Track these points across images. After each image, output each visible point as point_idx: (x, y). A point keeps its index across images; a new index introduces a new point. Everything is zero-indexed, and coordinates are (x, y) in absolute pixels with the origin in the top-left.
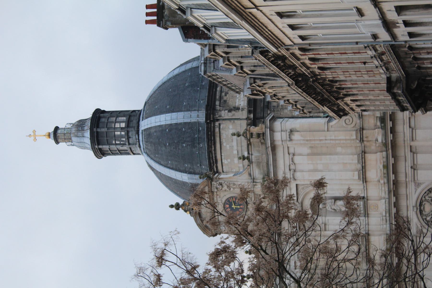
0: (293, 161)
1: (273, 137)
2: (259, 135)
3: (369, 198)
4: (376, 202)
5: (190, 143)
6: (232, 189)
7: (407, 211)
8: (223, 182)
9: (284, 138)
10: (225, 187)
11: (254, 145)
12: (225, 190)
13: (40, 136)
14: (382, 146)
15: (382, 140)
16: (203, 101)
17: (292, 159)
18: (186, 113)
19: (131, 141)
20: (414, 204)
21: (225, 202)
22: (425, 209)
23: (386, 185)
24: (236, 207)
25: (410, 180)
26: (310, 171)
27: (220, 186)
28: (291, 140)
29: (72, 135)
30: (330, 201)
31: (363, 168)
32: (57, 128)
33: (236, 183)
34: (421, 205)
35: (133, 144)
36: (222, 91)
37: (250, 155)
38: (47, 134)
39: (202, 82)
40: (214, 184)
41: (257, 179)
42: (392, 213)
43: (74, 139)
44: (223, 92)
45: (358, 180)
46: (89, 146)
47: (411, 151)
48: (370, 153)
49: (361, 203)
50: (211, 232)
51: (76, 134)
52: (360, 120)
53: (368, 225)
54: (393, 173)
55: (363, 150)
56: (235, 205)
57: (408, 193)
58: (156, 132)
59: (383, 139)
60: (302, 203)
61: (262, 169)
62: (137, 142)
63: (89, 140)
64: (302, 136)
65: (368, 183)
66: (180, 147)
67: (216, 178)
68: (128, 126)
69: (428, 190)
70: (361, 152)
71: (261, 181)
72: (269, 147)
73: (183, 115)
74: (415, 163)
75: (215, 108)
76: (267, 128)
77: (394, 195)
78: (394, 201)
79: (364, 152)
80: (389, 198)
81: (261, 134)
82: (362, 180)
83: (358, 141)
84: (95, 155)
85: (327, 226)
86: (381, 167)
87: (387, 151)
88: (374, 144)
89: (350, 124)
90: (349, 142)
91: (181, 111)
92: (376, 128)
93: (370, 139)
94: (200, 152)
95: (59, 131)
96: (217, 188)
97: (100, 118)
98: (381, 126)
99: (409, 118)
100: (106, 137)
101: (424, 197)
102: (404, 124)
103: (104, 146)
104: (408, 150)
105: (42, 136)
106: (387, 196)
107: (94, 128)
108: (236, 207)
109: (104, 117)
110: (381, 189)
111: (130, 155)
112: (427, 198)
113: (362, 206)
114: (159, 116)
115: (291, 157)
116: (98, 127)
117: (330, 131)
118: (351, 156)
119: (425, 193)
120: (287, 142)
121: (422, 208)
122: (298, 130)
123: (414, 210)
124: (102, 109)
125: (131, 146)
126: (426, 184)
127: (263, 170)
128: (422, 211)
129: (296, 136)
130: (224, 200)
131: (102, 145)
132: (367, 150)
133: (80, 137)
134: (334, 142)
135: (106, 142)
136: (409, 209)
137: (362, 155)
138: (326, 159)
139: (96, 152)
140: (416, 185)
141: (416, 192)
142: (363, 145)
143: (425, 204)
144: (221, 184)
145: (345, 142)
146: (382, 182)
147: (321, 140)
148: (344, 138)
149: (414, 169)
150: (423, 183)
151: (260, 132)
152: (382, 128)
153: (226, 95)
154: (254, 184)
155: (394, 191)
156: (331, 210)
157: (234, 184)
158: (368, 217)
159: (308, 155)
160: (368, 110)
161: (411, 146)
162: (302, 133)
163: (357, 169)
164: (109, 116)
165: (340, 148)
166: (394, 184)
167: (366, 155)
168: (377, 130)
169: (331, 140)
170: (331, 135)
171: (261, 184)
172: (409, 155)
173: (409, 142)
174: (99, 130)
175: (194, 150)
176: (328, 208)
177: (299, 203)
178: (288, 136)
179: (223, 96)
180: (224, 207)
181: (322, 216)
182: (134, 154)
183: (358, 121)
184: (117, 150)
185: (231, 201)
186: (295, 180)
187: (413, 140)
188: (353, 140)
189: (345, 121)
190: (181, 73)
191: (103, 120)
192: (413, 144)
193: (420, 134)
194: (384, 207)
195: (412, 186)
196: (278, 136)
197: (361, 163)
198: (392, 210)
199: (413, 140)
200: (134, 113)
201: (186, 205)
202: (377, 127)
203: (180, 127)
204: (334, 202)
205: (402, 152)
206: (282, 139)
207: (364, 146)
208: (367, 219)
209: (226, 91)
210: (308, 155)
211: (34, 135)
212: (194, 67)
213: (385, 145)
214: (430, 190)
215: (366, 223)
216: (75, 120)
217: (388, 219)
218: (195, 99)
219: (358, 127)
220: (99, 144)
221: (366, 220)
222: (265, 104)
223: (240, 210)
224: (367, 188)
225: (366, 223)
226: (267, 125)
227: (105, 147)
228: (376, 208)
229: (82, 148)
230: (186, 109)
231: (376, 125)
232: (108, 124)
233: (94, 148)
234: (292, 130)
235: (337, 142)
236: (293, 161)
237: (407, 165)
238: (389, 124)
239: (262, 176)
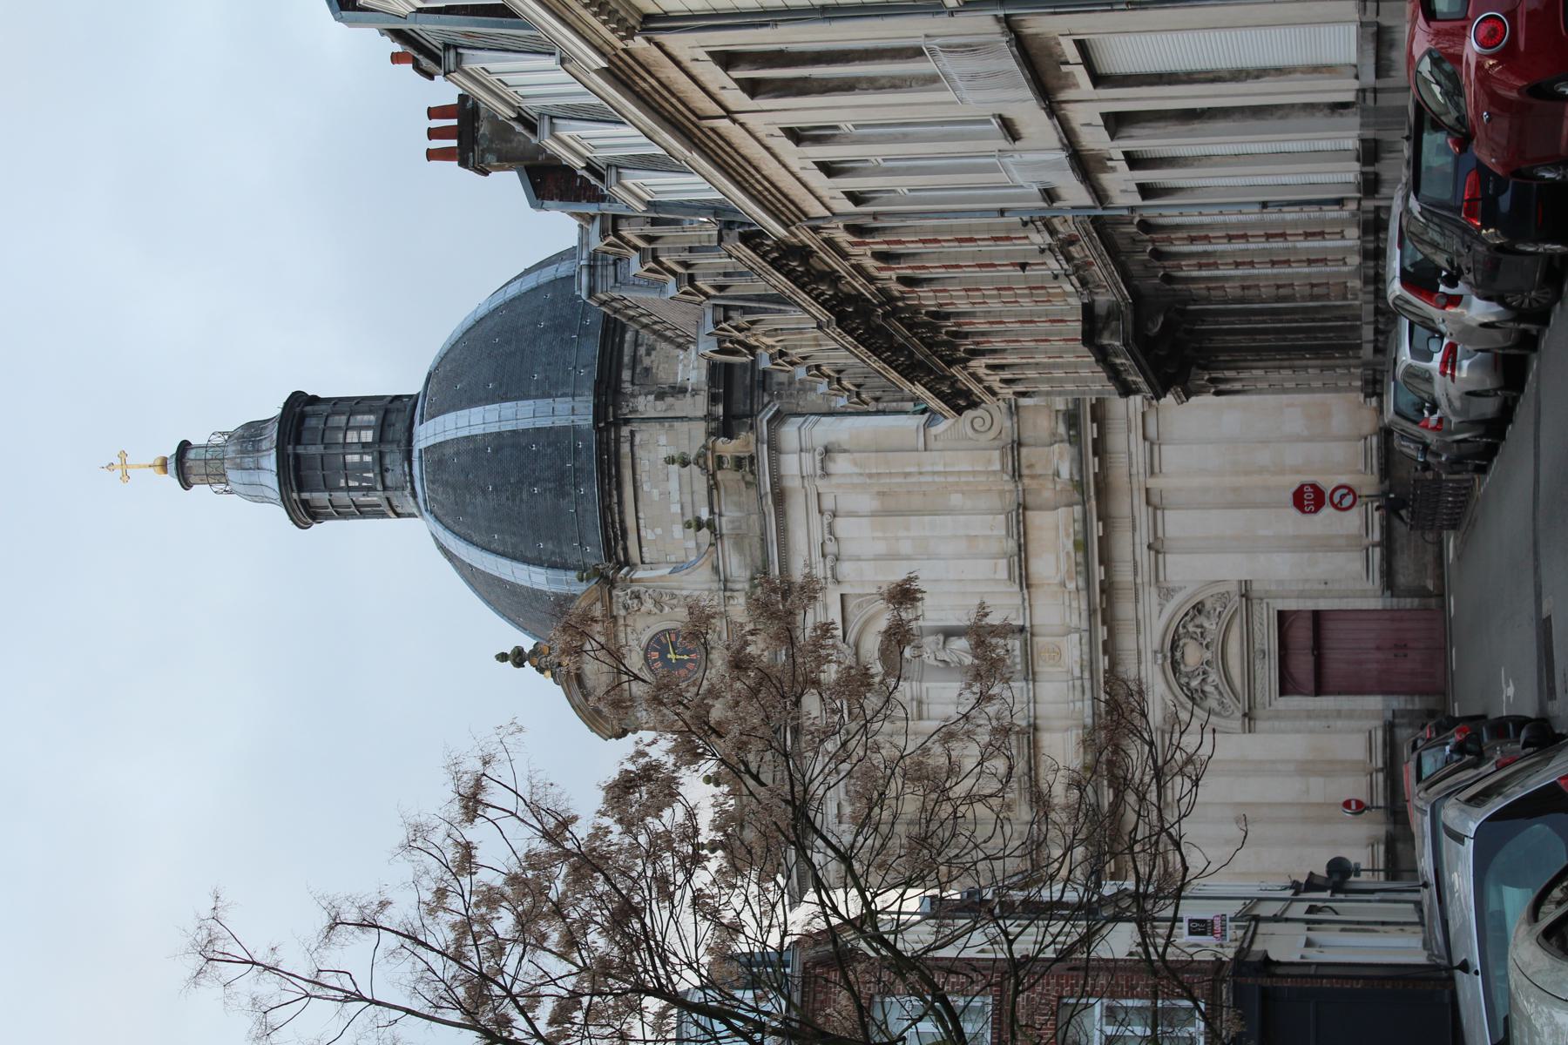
0: (831, 533)
1: (778, 465)
2: (738, 463)
3: (1036, 630)
4: (1057, 640)
5: (551, 485)
6: (667, 609)
7: (1139, 663)
8: (643, 590)
9: (808, 470)
10: (649, 605)
11: (725, 488)
12: (649, 613)
13: (139, 466)
14: (1070, 488)
15: (1071, 474)
16: (588, 369)
17: (830, 525)
18: (540, 402)
19: (389, 478)
20: (1156, 646)
21: (648, 645)
22: (1186, 657)
23: (1083, 594)
24: (678, 657)
25: (1146, 579)
26: (877, 558)
27: (636, 601)
28: (826, 474)
29: (226, 466)
30: (932, 638)
31: (1020, 550)
32: (184, 446)
33: (676, 592)
34: (1174, 647)
35: (396, 489)
36: (640, 342)
37: (717, 517)
38: (158, 462)
39: (584, 317)
40: (618, 596)
41: (734, 582)
42: (1098, 669)
43: (232, 475)
44: (642, 345)
45: (1008, 583)
46: (276, 495)
47: (1148, 503)
48: (1040, 508)
49: (1015, 644)
50: (610, 727)
51: (238, 461)
52: (1012, 419)
53: (1035, 702)
54: (1101, 562)
55: (1021, 501)
56: (675, 654)
57: (1141, 616)
58: (457, 454)
59: (1075, 472)
60: (857, 646)
61: (748, 553)
62: (406, 482)
63: (276, 479)
64: (856, 464)
65: (1033, 590)
66: (525, 496)
67: (623, 580)
68: (381, 438)
69: (1194, 607)
70: (1015, 507)
71: (747, 586)
72: (766, 494)
73: (532, 408)
74: (1160, 534)
75: (621, 388)
76: (763, 443)
77: (1104, 622)
78: (1103, 635)
79: (1023, 507)
80: (1091, 630)
81: (745, 458)
82: (1017, 581)
83: (1006, 477)
84: (292, 519)
85: (925, 707)
86: (1070, 546)
87: (1084, 504)
88: (1050, 486)
89: (986, 432)
90: (983, 478)
91: (527, 397)
92: (1056, 442)
93: (1038, 470)
94: (580, 509)
95: (191, 454)
96: (626, 607)
97: (303, 417)
98: (1069, 436)
99: (1144, 414)
100: (320, 468)
101: (1184, 627)
102: (1129, 430)
103: (316, 495)
104: (1139, 500)
105: (145, 466)
106: (1085, 625)
107: (289, 444)
108: (678, 657)
109: (315, 414)
110: (1070, 605)
111: (390, 517)
112: (1191, 628)
113: (1017, 652)
114: (466, 412)
115: (826, 522)
116: (298, 442)
117: (931, 450)
118: (991, 517)
119: (1186, 614)
120: (817, 479)
121: (1178, 655)
122: (846, 447)
123: (1155, 662)
124: (310, 394)
125: (389, 494)
126: (1189, 590)
127: (751, 555)
128: (1179, 664)
129: (840, 464)
130: (645, 639)
131: (311, 491)
132: (1030, 500)
133: (250, 469)
134: (942, 479)
135: (322, 483)
136: (1143, 659)
137: (1018, 515)
138: (921, 527)
139: (294, 510)
141: (1160, 612)
142: (1020, 488)
143: (1185, 645)
144: (637, 596)
145: (972, 479)
146: (1071, 586)
147: (907, 475)
148: (970, 469)
149: (1157, 552)
150: (1181, 589)
151: (742, 455)
152: (1070, 443)
153: (648, 354)
154: (728, 594)
155: (1103, 611)
156: (936, 663)
157: (673, 596)
158: (1034, 681)
159: (874, 514)
160: (1034, 392)
161: (1147, 490)
162: (856, 455)
163: (1005, 554)
164: (330, 411)
165: (959, 496)
166: (1102, 591)
167: (1029, 513)
168: (1056, 446)
169: (934, 473)
170: (934, 462)
171: (746, 593)
172: (1143, 513)
173: (1142, 478)
174: (301, 450)
175: (563, 503)
176: (928, 658)
177: (848, 644)
178: (818, 465)
179: (641, 356)
180: (646, 659)
181: (912, 680)
182: (398, 515)
183: (1008, 424)
184: (351, 503)
185: (664, 641)
186: (839, 582)
187: (1152, 473)
188: (994, 472)
189: (972, 422)
190: (525, 293)
191: (312, 422)
192: (1152, 483)
193: (1171, 456)
194: (1077, 653)
195: (1150, 597)
196: (791, 465)
197: (1015, 537)
198: (1097, 662)
199: (1152, 473)
200: (397, 404)
201: (543, 653)
202: (1058, 439)
203: (523, 441)
204: (944, 643)
205: (1128, 505)
206: (801, 472)
207: (1024, 490)
208: (1031, 686)
209: (650, 343)
210: (874, 514)
211: (122, 466)
212: (562, 278)
213: (1080, 486)
214: (1200, 606)
215: (1029, 698)
216: (232, 425)
217: (1087, 685)
218: (564, 364)
219: (1007, 438)
220: (300, 490)
221: (1028, 690)
222: (756, 378)
223: (690, 665)
224: (1033, 603)
225: (1029, 698)
226: (762, 433)
227: (320, 498)
228: (1057, 658)
229: (256, 499)
230: (540, 392)
231: (1054, 434)
232: (327, 432)
233: (289, 499)
234: (829, 447)
235: (950, 479)
236: (831, 533)
237: (1137, 540)
238: (1091, 431)
239: (748, 574)
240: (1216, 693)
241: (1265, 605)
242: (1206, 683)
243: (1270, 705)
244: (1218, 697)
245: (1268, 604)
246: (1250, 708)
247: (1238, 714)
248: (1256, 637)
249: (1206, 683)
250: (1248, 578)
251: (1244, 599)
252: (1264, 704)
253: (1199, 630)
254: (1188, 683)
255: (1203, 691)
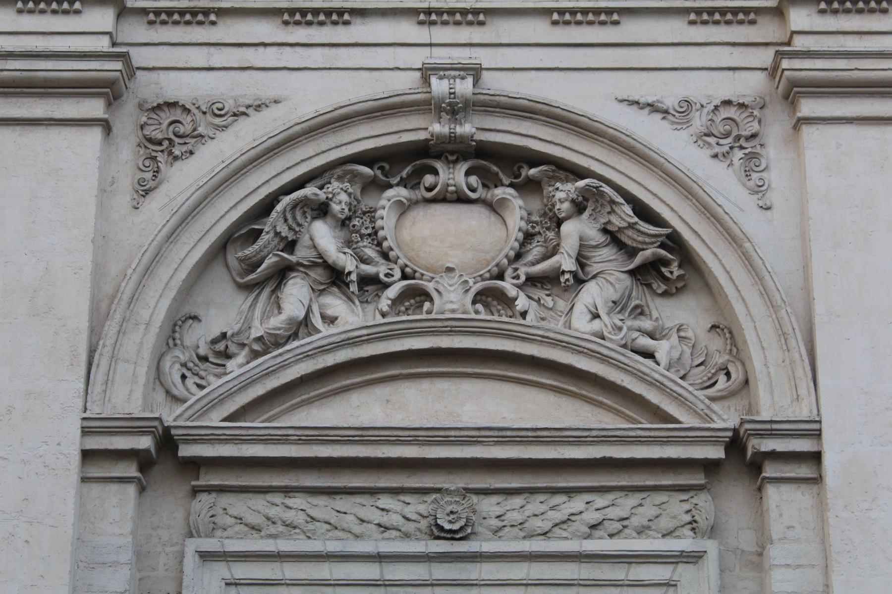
22: (441, 211)
140: (732, 112)
141: (653, 108)
143: (494, 207)
150: (759, 190)
240: (276, 322)
241: (685, 543)
242: (319, 292)
243: (206, 556)
244: (256, 333)
245: (694, 558)
246: (196, 465)
247: (170, 415)
248: (536, 504)
249: (319, 292)
250: (829, 461)
251: (716, 453)
252: (214, 529)
253: (568, 264)
254: (322, 210)
255: (282, 273)
